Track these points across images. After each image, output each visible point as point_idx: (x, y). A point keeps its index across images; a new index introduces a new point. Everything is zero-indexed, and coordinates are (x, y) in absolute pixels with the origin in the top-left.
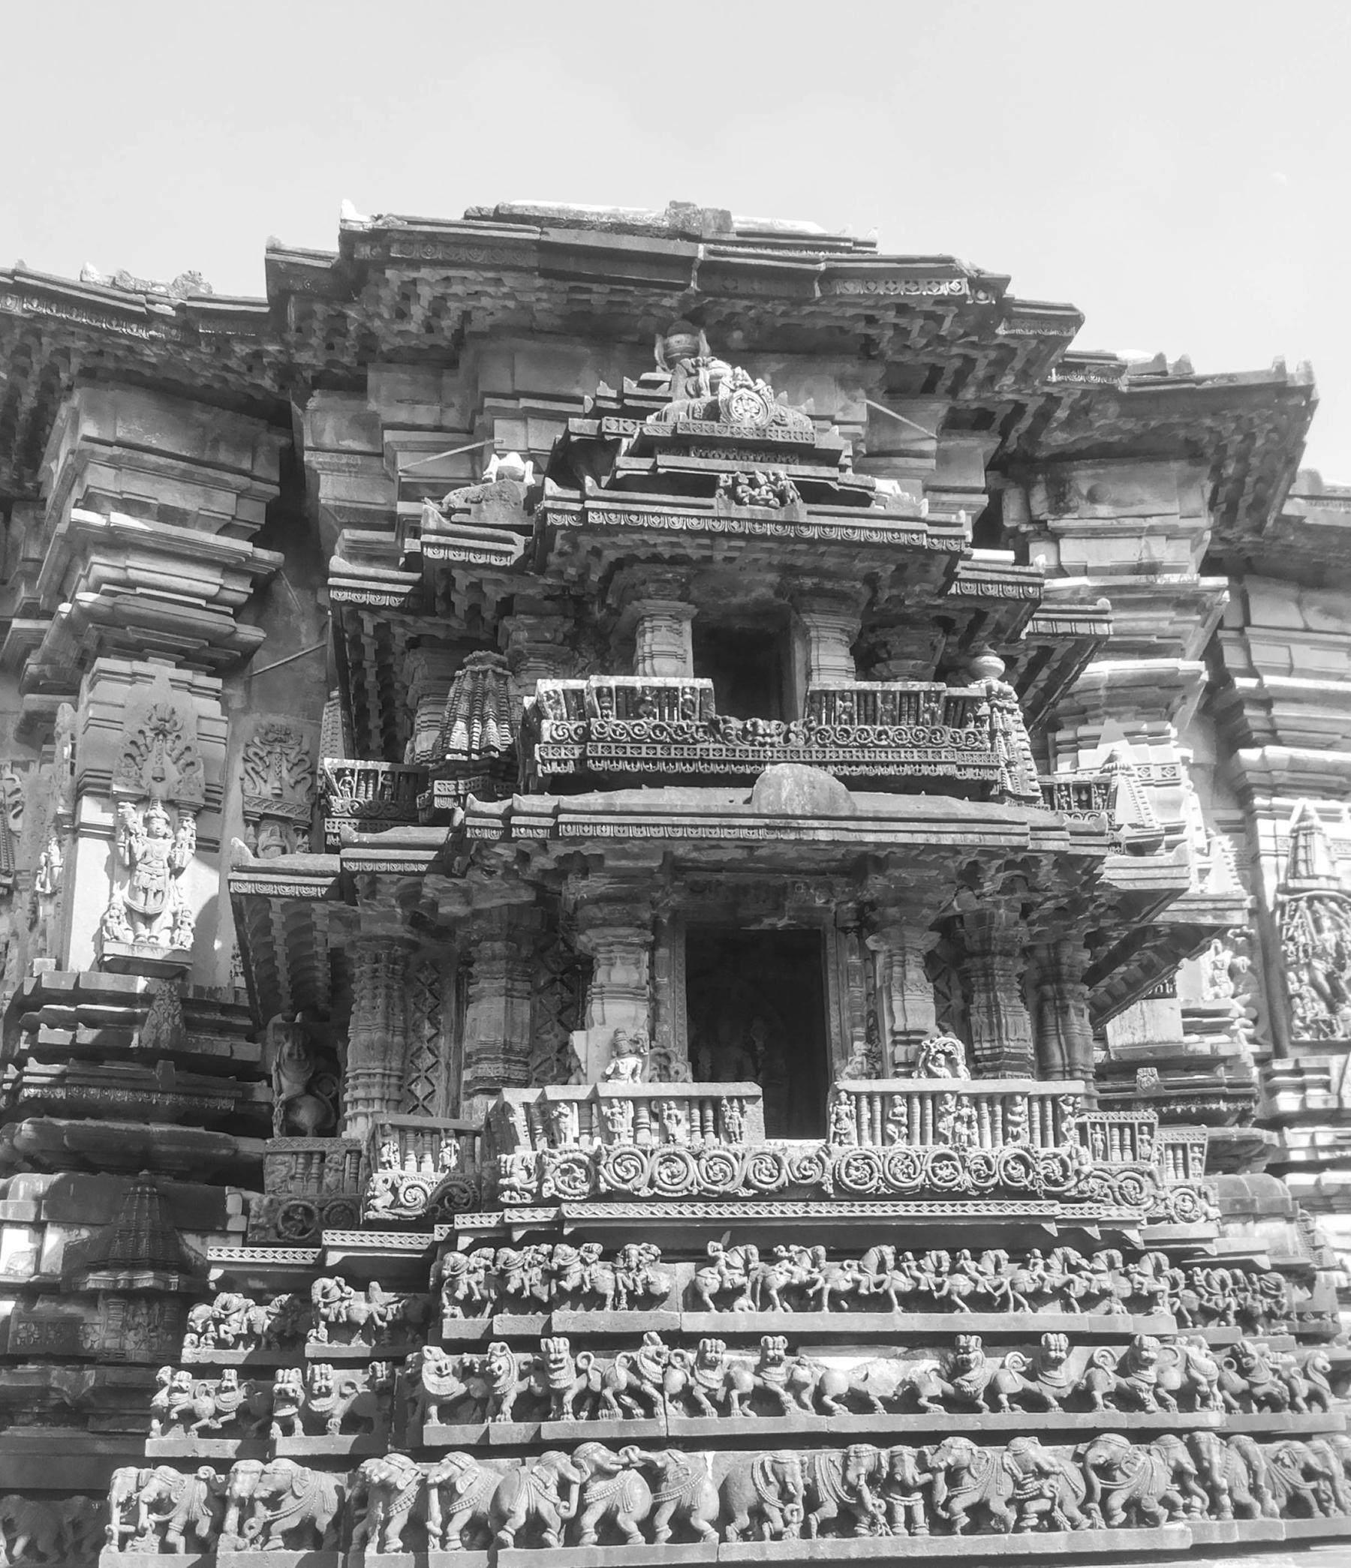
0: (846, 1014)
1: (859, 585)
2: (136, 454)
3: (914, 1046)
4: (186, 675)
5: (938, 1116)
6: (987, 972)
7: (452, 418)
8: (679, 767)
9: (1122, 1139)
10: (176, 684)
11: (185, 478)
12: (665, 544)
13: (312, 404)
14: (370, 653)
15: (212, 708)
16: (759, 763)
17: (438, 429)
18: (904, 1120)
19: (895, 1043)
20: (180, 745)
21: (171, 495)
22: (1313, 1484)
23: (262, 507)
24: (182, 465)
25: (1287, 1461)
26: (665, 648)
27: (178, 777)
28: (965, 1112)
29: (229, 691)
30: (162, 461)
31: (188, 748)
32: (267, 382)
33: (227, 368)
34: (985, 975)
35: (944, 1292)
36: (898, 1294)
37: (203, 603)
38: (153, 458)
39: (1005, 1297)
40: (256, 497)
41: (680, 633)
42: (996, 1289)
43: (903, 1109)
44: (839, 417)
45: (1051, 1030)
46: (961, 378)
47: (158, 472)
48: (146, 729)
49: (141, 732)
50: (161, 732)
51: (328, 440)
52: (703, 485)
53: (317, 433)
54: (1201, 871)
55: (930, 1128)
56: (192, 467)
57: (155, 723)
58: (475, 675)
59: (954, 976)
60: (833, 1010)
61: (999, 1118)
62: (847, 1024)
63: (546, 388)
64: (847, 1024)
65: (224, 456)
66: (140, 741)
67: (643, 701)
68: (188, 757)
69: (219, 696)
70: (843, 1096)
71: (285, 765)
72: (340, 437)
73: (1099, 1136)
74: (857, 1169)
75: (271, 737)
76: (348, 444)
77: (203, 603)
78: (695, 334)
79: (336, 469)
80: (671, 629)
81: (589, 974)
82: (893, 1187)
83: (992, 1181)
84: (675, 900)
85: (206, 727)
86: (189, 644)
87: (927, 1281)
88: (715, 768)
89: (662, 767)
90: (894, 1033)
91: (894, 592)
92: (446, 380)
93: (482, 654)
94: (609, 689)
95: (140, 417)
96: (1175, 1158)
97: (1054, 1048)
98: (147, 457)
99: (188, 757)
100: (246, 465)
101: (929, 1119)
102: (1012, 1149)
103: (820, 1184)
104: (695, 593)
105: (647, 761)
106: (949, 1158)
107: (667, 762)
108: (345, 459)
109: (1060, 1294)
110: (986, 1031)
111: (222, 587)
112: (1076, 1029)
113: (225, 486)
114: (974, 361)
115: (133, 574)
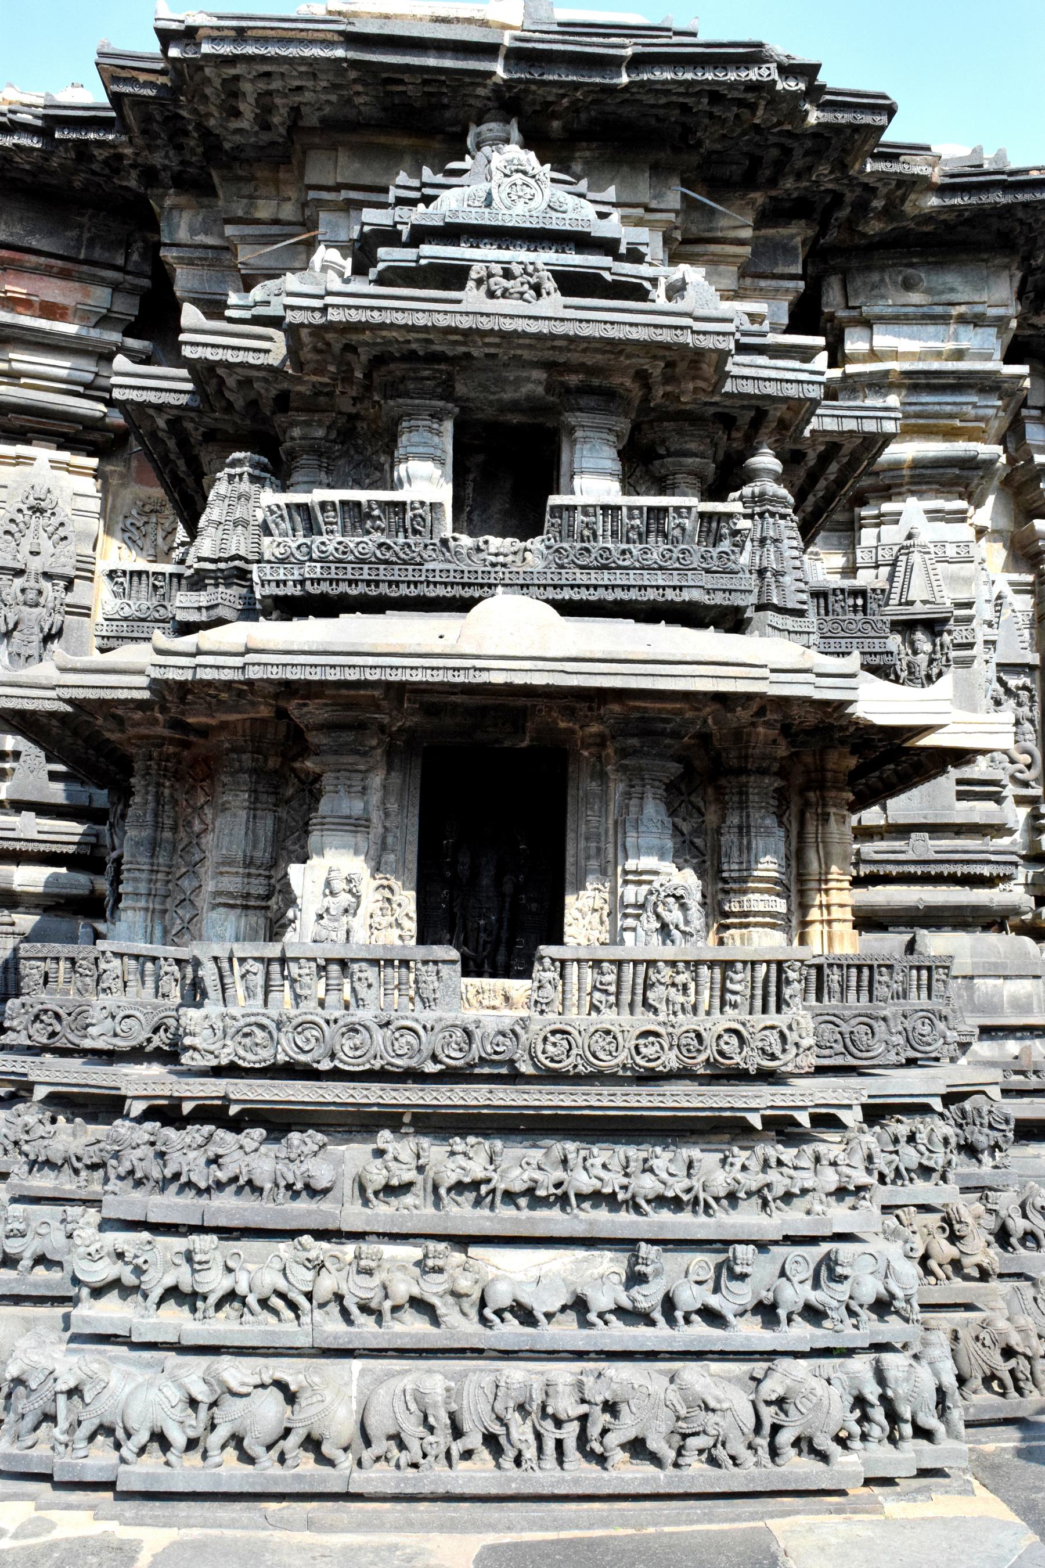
0: (582, 844)
1: (628, 383)
2: (17, 255)
3: (645, 888)
4: (65, 456)
5: (647, 986)
6: (743, 792)
7: (288, 211)
8: (404, 590)
9: (859, 979)
10: (55, 465)
11: (64, 275)
12: (417, 340)
13: (168, 202)
14: (171, 444)
15: (90, 485)
16: (490, 586)
17: (276, 222)
18: (612, 989)
19: (626, 882)
20: (55, 521)
21: (53, 291)
22: (1012, 1363)
23: (136, 301)
24: (59, 263)
25: (988, 1342)
26: (421, 450)
27: (52, 550)
28: (683, 978)
29: (109, 468)
30: (42, 260)
31: (62, 524)
32: (133, 183)
33: (94, 173)
34: (741, 793)
35: (629, 1195)
36: (578, 1196)
37: (81, 389)
38: (33, 259)
39: (696, 1198)
40: (132, 291)
41: (439, 434)
42: (689, 1191)
43: (613, 978)
44: (654, 205)
45: (811, 838)
46: (780, 167)
47: (47, 272)
48: (24, 507)
49: (20, 511)
50: (37, 510)
51: (183, 235)
52: (453, 276)
53: (173, 229)
54: (986, 642)
55: (639, 998)
56: (69, 265)
57: (32, 502)
58: (231, 478)
59: (710, 791)
60: (570, 836)
61: (718, 986)
62: (582, 855)
63: (367, 180)
64: (582, 855)
65: (98, 254)
66: (19, 518)
67: (369, 516)
68: (62, 532)
69: (97, 474)
70: (547, 962)
71: (160, 534)
72: (193, 232)
73: (836, 978)
74: (554, 1044)
75: (147, 508)
76: (201, 239)
77: (81, 389)
78: (508, 122)
79: (190, 262)
80: (430, 430)
81: (316, 797)
82: (592, 1064)
83: (703, 1057)
84: (411, 721)
85: (81, 503)
86: (66, 428)
87: (613, 1182)
88: (441, 591)
89: (384, 589)
90: (626, 872)
91: (669, 388)
92: (281, 175)
93: (237, 455)
94: (333, 503)
95: (21, 220)
96: (919, 979)
97: (812, 857)
98: (27, 257)
99: (62, 532)
100: (120, 261)
101: (640, 990)
102: (730, 1019)
103: (511, 1062)
104: (460, 389)
105: (368, 583)
106: (657, 1035)
107: (390, 583)
108: (198, 253)
109: (762, 1197)
110: (735, 853)
111: (97, 374)
112: (835, 837)
113: (102, 282)
114: (791, 150)
115: (16, 365)
